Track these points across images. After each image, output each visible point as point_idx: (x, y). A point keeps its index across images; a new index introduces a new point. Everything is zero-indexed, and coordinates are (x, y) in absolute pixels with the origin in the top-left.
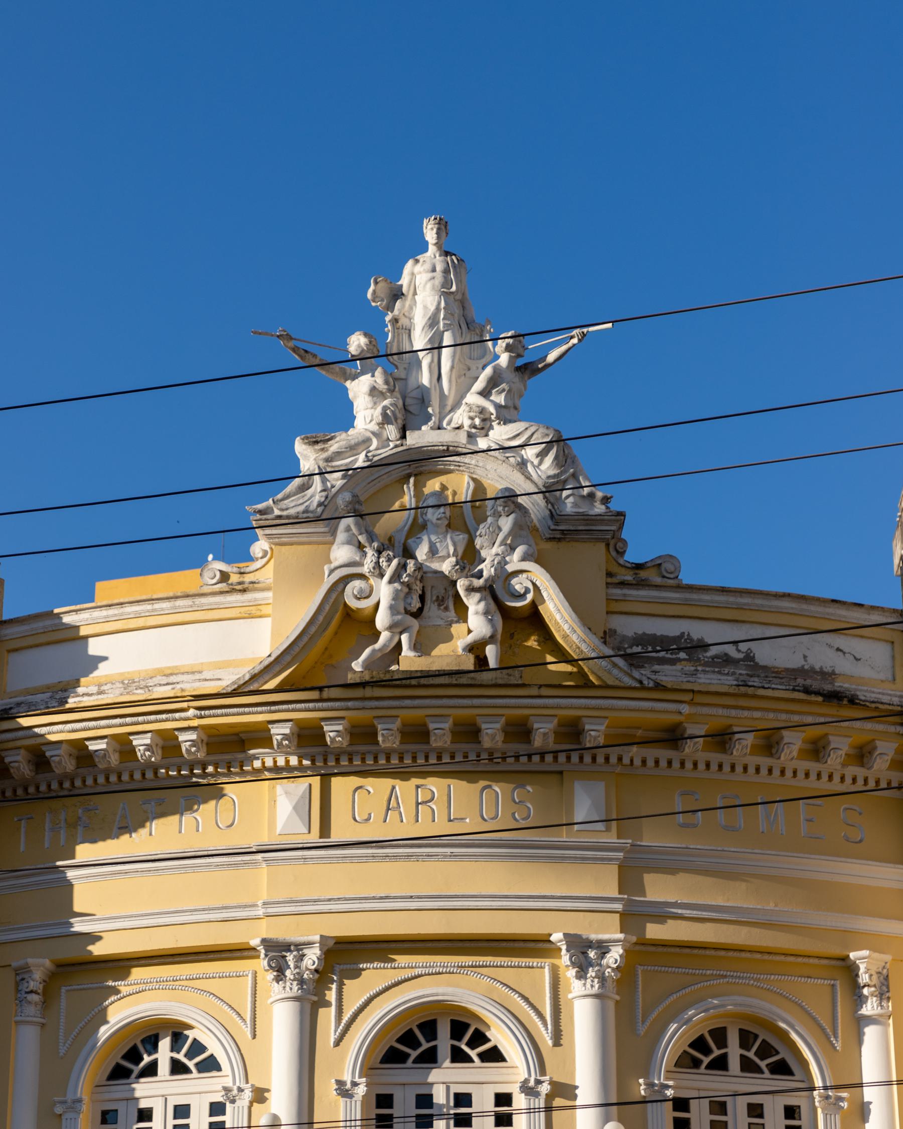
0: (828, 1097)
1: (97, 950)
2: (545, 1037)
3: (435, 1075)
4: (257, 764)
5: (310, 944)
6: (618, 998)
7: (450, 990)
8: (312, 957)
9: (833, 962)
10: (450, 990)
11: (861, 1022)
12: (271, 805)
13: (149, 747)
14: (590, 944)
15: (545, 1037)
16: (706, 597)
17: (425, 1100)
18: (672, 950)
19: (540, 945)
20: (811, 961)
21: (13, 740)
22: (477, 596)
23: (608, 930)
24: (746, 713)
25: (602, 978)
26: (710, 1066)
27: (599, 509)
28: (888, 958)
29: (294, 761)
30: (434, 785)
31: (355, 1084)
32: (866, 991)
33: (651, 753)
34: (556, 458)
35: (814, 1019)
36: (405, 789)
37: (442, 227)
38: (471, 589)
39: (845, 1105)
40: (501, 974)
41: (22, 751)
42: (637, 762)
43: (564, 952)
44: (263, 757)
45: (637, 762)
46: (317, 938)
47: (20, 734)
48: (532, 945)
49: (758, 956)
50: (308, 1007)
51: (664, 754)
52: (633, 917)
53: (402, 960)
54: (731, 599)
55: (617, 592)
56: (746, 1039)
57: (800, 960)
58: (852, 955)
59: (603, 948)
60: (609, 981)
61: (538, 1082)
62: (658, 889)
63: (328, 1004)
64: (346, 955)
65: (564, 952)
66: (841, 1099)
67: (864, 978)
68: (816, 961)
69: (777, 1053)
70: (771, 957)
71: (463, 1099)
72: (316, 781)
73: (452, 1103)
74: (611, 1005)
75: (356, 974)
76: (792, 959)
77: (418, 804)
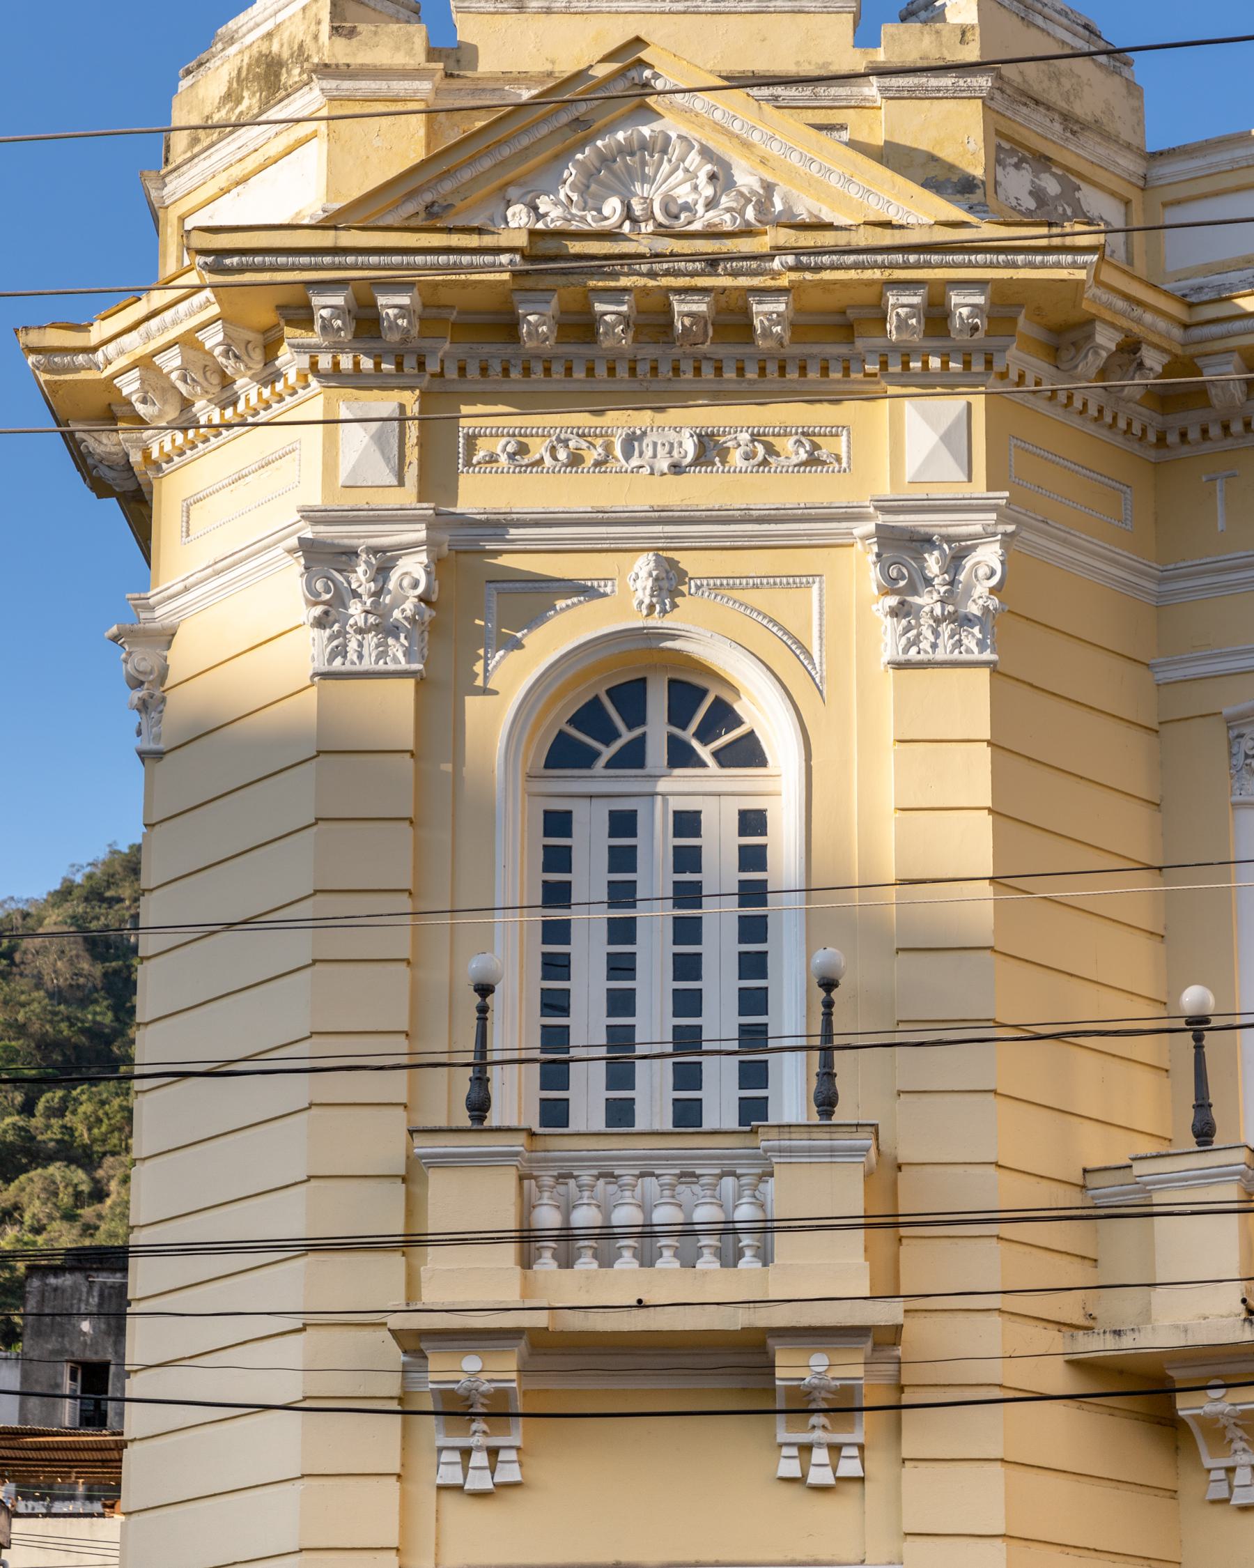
21: (1222, 337)
41: (1236, 357)
47: (1238, 325)
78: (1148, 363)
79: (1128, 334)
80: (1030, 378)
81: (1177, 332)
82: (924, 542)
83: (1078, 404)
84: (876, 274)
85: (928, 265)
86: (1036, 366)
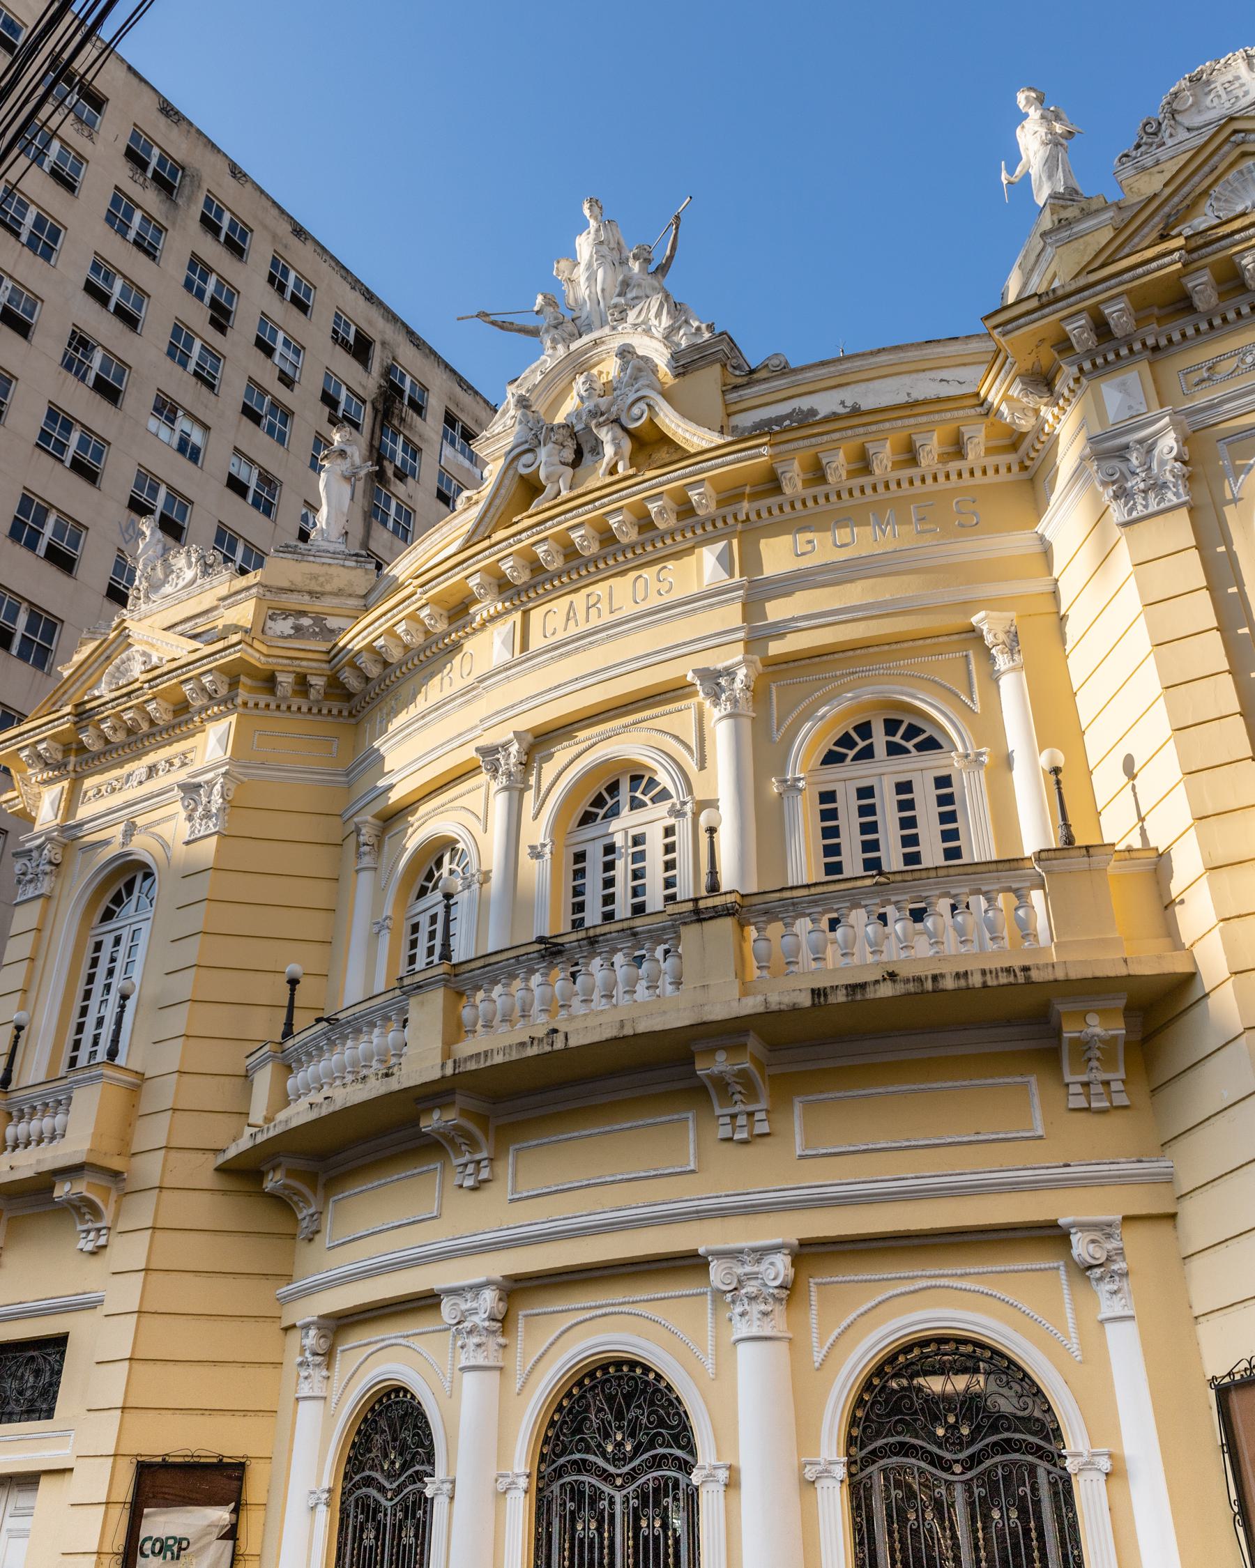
0: (967, 756)
1: (394, 796)
2: (691, 765)
3: (615, 825)
4: (478, 618)
5: (510, 741)
6: (754, 715)
7: (617, 747)
8: (514, 749)
9: (964, 636)
10: (617, 747)
11: (993, 678)
12: (489, 646)
13: (407, 632)
14: (719, 674)
15: (691, 765)
16: (809, 374)
17: (610, 849)
18: (803, 662)
19: (687, 690)
20: (941, 639)
22: (605, 429)
23: (733, 656)
24: (825, 438)
25: (735, 702)
26: (855, 758)
27: (707, 335)
28: (1013, 615)
29: (500, 606)
30: (600, 589)
31: (544, 845)
32: (993, 651)
33: (763, 503)
34: (668, 312)
35: (949, 690)
36: (579, 599)
37: (594, 202)
38: (599, 425)
39: (985, 759)
40: (659, 723)
41: (347, 668)
42: (753, 517)
43: (699, 688)
44: (481, 611)
45: (753, 517)
46: (511, 735)
48: (680, 692)
49: (887, 647)
50: (516, 794)
51: (773, 501)
52: (756, 639)
53: (582, 735)
54: (832, 369)
55: (733, 396)
56: (891, 726)
57: (929, 641)
58: (974, 620)
59: (729, 672)
60: (742, 703)
61: (684, 803)
62: (776, 610)
63: (530, 787)
64: (541, 742)
65: (699, 688)
66: (981, 754)
67: (989, 639)
68: (946, 638)
69: (924, 731)
70: (899, 646)
71: (638, 840)
72: (517, 616)
73: (630, 843)
74: (747, 724)
75: (551, 756)
76: (921, 642)
77: (588, 608)
78: (313, 682)
79: (298, 674)
80: (262, 705)
81: (325, 666)
82: (200, 786)
83: (294, 708)
84: (175, 681)
85: (190, 671)
86: (263, 699)
